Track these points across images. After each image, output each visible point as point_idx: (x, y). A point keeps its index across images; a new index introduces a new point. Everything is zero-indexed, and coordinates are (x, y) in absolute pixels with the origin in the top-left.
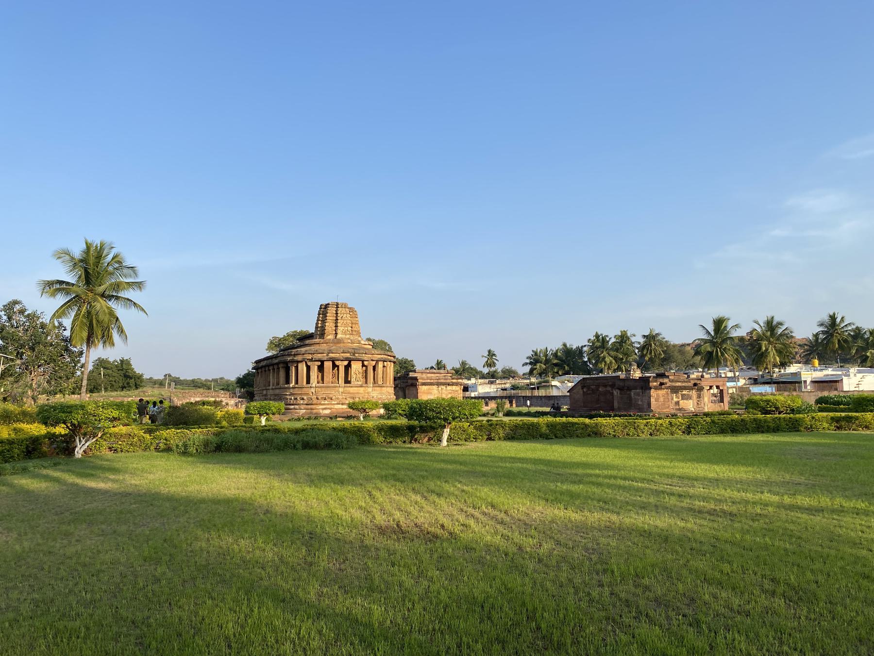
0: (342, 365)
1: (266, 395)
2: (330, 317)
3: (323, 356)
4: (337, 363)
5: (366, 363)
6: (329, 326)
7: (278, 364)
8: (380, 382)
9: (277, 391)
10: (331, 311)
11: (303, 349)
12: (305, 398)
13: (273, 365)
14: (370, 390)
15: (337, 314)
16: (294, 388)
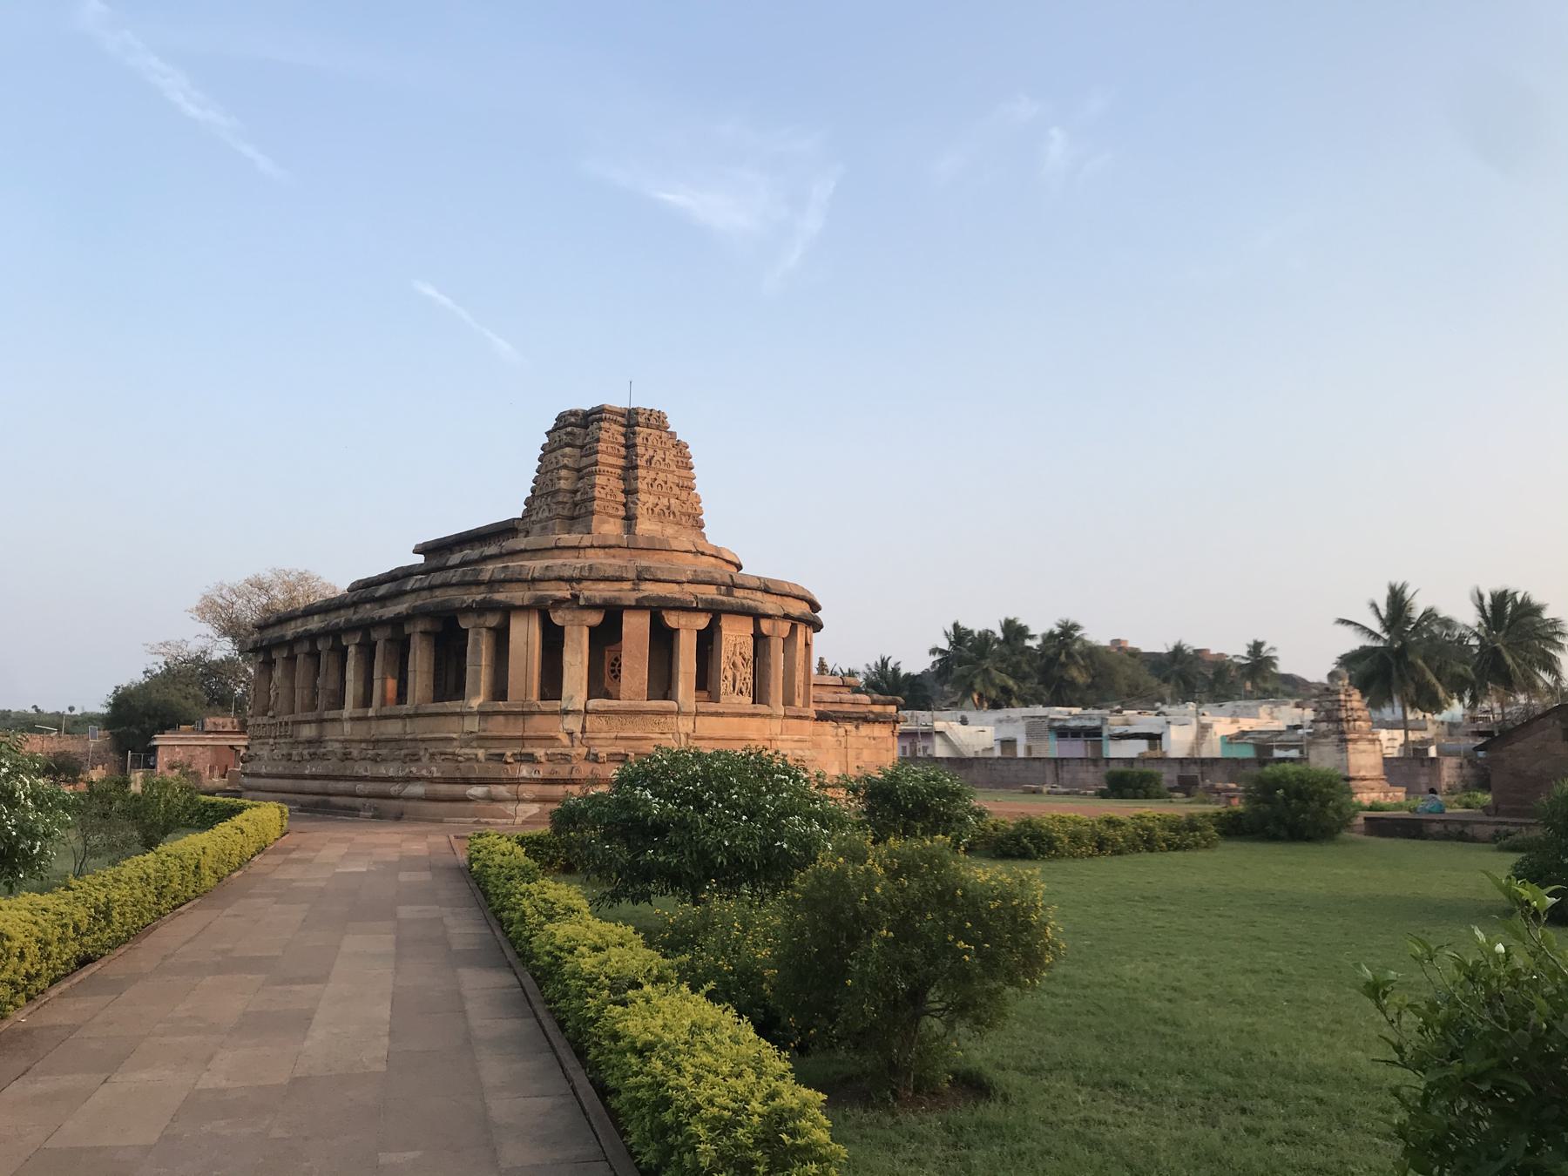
0: (688, 629)
1: (318, 741)
2: (609, 456)
3: (624, 592)
4: (672, 620)
5: (765, 625)
6: (606, 485)
7: (398, 622)
8: (799, 702)
9: (393, 728)
10: (611, 434)
11: (535, 566)
12: (540, 753)
13: (366, 627)
14: (775, 726)
15: (630, 446)
16: (483, 714)
